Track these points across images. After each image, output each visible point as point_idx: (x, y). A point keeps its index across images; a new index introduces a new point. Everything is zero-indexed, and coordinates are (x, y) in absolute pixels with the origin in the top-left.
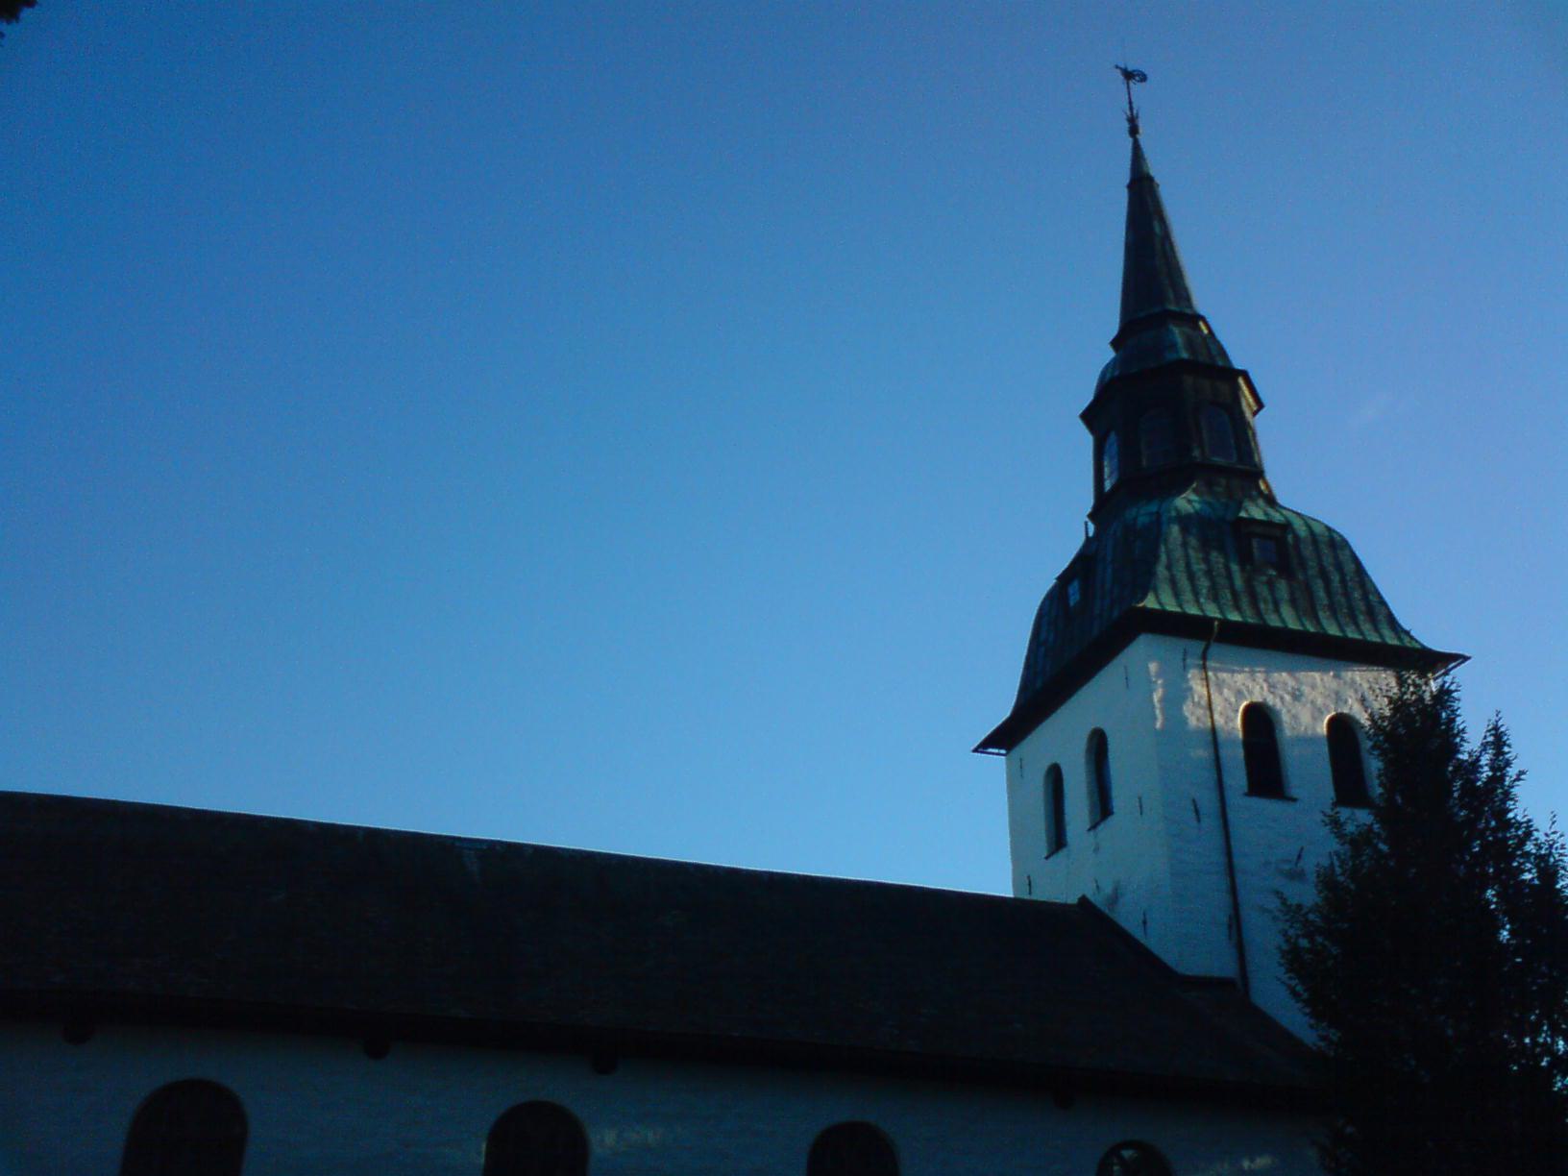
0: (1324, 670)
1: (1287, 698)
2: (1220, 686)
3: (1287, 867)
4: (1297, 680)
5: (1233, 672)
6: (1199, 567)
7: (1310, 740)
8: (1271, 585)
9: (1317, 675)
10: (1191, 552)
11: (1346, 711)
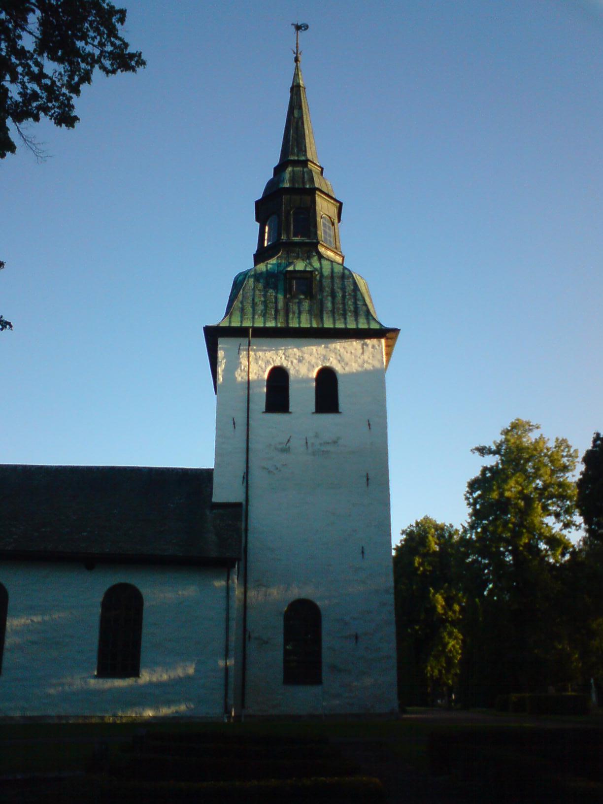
0: (319, 345)
1: (295, 361)
2: (257, 360)
3: (280, 447)
5: (265, 351)
6: (259, 299)
7: (307, 380)
8: (300, 303)
9: (314, 348)
10: (257, 292)
11: (328, 365)
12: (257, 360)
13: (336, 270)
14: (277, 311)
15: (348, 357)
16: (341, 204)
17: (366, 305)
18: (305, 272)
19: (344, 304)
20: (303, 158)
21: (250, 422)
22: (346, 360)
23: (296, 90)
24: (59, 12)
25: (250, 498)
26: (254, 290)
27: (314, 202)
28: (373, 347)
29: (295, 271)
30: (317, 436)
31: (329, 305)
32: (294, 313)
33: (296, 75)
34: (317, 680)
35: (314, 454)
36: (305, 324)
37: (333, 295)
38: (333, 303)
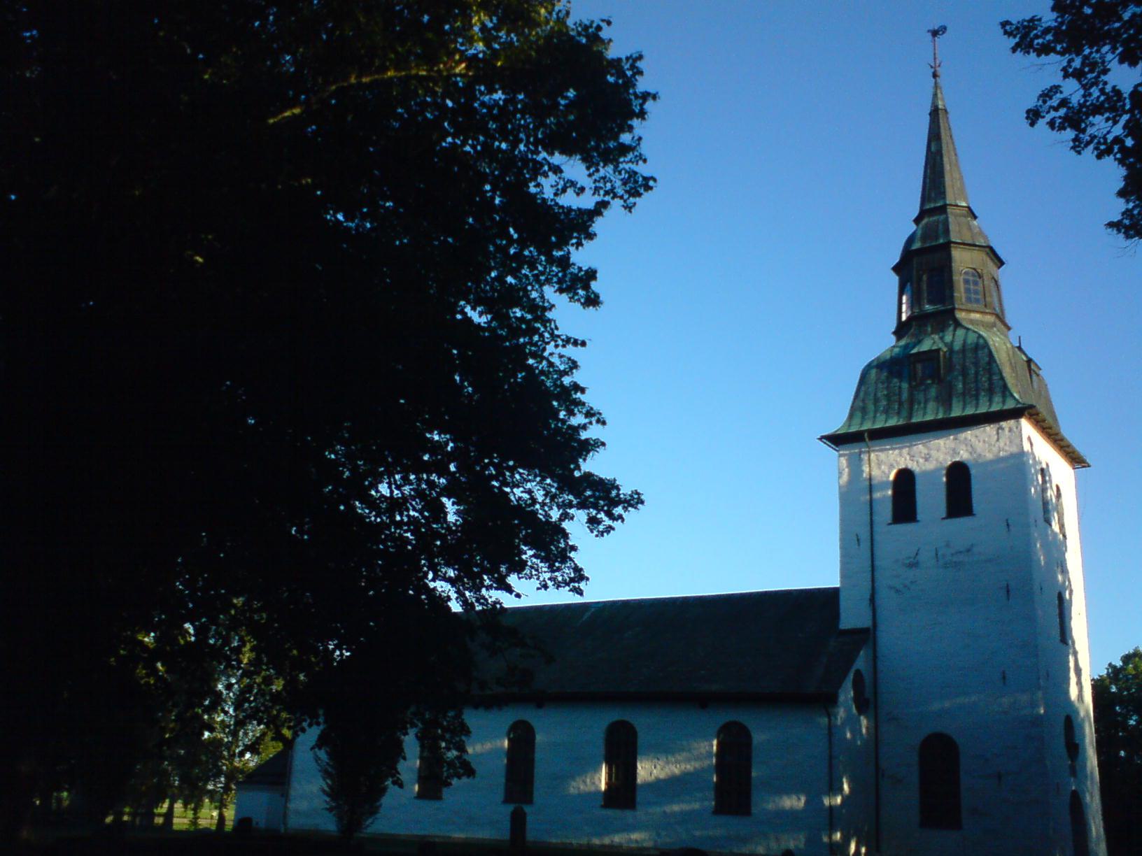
1: (921, 461)
2: (879, 464)
4: (929, 449)
8: (928, 388)
11: (957, 459)
13: (969, 341)
14: (901, 404)
15: (976, 446)
16: (991, 248)
17: (1002, 378)
18: (930, 351)
19: (976, 381)
21: (877, 537)
22: (979, 450)
23: (935, 113)
25: (880, 620)
27: (949, 258)
28: (1010, 430)
29: (919, 353)
30: (948, 546)
31: (960, 386)
32: (919, 403)
33: (935, 95)
34: (957, 825)
35: (946, 566)
36: (929, 417)
37: (964, 373)
38: (964, 384)
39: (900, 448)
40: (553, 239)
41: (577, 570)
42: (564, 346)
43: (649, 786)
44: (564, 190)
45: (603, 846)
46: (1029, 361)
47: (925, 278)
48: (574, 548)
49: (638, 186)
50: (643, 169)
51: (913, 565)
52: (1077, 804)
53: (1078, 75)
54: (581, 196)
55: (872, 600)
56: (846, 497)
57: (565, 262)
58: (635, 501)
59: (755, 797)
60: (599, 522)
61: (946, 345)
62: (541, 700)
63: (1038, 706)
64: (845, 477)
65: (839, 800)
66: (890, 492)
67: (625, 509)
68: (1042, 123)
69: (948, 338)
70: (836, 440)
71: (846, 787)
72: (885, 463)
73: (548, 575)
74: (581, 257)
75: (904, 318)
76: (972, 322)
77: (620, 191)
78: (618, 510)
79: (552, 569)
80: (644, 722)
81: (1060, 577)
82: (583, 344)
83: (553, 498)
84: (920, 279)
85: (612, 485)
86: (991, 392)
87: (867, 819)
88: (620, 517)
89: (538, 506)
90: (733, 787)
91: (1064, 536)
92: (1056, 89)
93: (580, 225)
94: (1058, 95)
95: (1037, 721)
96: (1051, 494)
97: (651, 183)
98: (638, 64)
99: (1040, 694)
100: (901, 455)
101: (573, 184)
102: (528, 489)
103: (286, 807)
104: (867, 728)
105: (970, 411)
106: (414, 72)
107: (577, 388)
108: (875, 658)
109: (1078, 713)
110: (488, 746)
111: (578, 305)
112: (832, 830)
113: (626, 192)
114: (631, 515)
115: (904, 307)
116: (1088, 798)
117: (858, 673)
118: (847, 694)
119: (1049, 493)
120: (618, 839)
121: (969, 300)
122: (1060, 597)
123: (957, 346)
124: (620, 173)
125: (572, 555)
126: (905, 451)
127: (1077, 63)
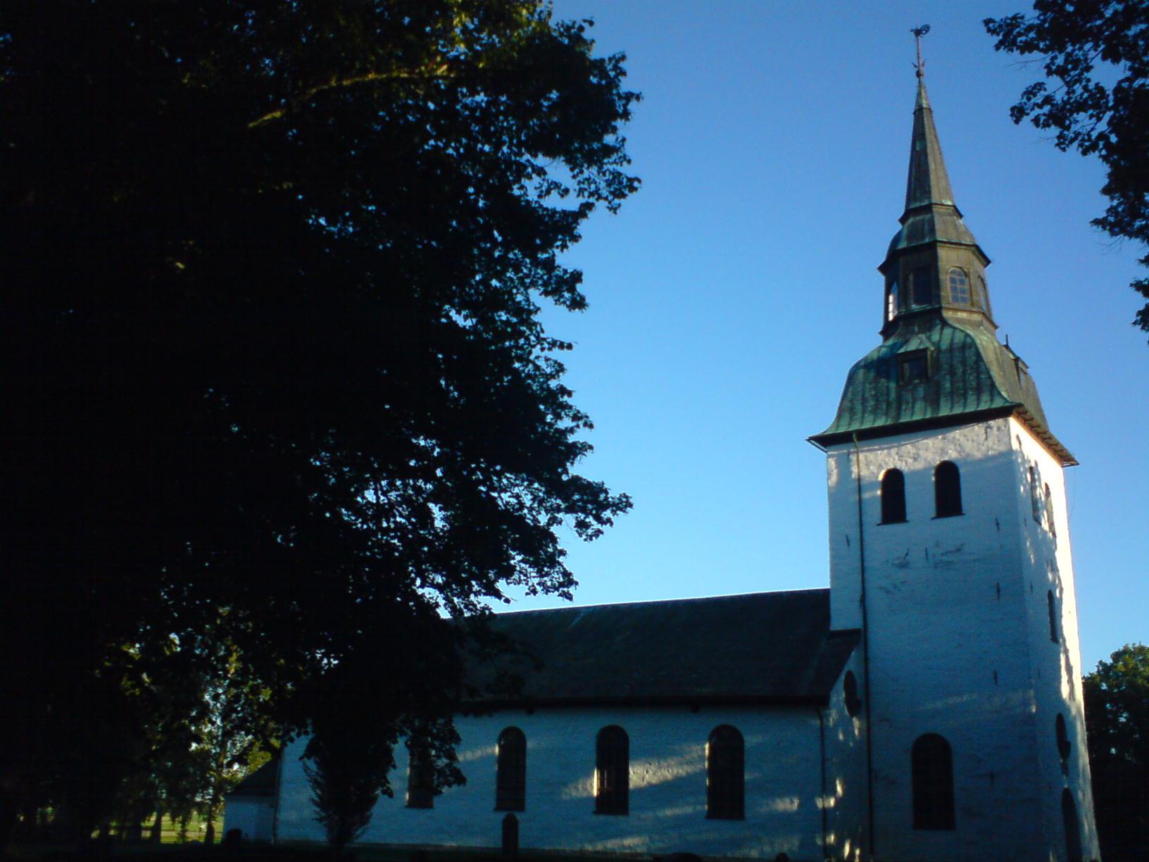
0: (936, 435)
1: (910, 461)
2: (868, 465)
8: (916, 386)
12: (868, 465)
13: (956, 340)
14: (888, 404)
15: (965, 444)
16: (977, 247)
17: (990, 378)
19: (964, 381)
20: (926, 202)
21: (865, 537)
24: (455, 389)
25: (870, 621)
26: (864, 383)
27: (935, 258)
28: (999, 429)
30: (937, 545)
31: (948, 385)
32: (907, 403)
33: (919, 94)
35: (936, 566)
36: (917, 417)
37: (952, 373)
38: (952, 383)
39: (888, 448)
40: (538, 241)
41: (566, 574)
42: (550, 349)
43: (640, 791)
44: (548, 192)
45: (597, 852)
46: (1017, 359)
47: (911, 278)
48: (562, 553)
49: (622, 187)
50: (627, 170)
51: (904, 565)
52: (1069, 801)
53: (1061, 72)
54: (567, 198)
55: (863, 600)
56: (835, 498)
57: (550, 265)
58: (623, 504)
59: (748, 799)
60: (587, 526)
61: (933, 344)
62: (531, 706)
63: (1029, 705)
64: (834, 478)
65: (832, 802)
66: (879, 492)
67: (614, 512)
68: (1026, 120)
69: (935, 337)
70: (825, 441)
71: (839, 789)
72: (874, 463)
73: (536, 580)
74: (567, 259)
75: (891, 317)
76: (959, 321)
77: (604, 193)
78: (607, 514)
79: (541, 574)
80: (635, 727)
81: (1050, 576)
82: (570, 347)
83: (541, 502)
84: (906, 278)
85: (600, 489)
86: (979, 391)
87: (860, 819)
88: (609, 521)
89: (526, 511)
90: (726, 790)
91: (1054, 534)
92: (1040, 86)
93: (564, 227)
94: (1042, 93)
95: (1030, 720)
96: (1040, 492)
97: (636, 184)
98: (621, 64)
99: (1032, 693)
100: (889, 455)
101: (557, 185)
102: (515, 494)
103: (276, 819)
104: (860, 729)
105: (958, 410)
106: (395, 74)
107: (563, 391)
108: (866, 660)
109: (1069, 710)
110: (479, 753)
111: (563, 308)
112: (825, 832)
113: (611, 193)
114: (619, 518)
115: (891, 307)
116: (1080, 795)
117: (850, 674)
118: (838, 696)
119: (1038, 491)
120: (611, 844)
121: (955, 299)
122: (1051, 595)
123: (944, 346)
124: (604, 174)
125: (561, 559)
126: (893, 451)
127: (1060, 60)
